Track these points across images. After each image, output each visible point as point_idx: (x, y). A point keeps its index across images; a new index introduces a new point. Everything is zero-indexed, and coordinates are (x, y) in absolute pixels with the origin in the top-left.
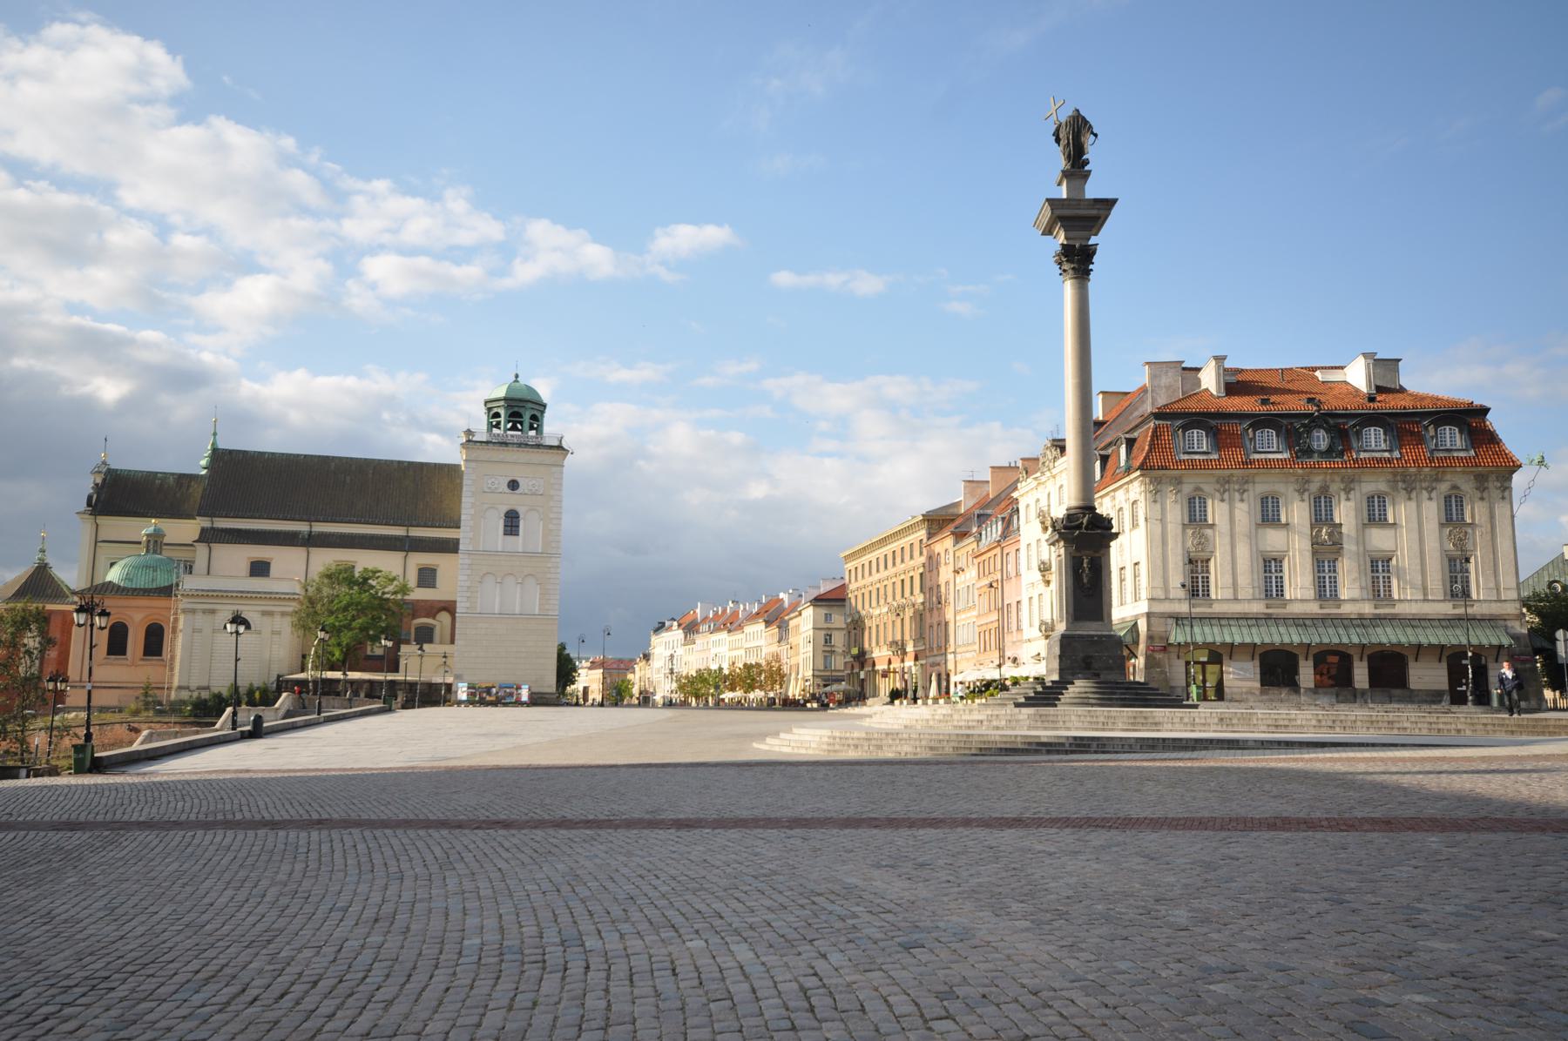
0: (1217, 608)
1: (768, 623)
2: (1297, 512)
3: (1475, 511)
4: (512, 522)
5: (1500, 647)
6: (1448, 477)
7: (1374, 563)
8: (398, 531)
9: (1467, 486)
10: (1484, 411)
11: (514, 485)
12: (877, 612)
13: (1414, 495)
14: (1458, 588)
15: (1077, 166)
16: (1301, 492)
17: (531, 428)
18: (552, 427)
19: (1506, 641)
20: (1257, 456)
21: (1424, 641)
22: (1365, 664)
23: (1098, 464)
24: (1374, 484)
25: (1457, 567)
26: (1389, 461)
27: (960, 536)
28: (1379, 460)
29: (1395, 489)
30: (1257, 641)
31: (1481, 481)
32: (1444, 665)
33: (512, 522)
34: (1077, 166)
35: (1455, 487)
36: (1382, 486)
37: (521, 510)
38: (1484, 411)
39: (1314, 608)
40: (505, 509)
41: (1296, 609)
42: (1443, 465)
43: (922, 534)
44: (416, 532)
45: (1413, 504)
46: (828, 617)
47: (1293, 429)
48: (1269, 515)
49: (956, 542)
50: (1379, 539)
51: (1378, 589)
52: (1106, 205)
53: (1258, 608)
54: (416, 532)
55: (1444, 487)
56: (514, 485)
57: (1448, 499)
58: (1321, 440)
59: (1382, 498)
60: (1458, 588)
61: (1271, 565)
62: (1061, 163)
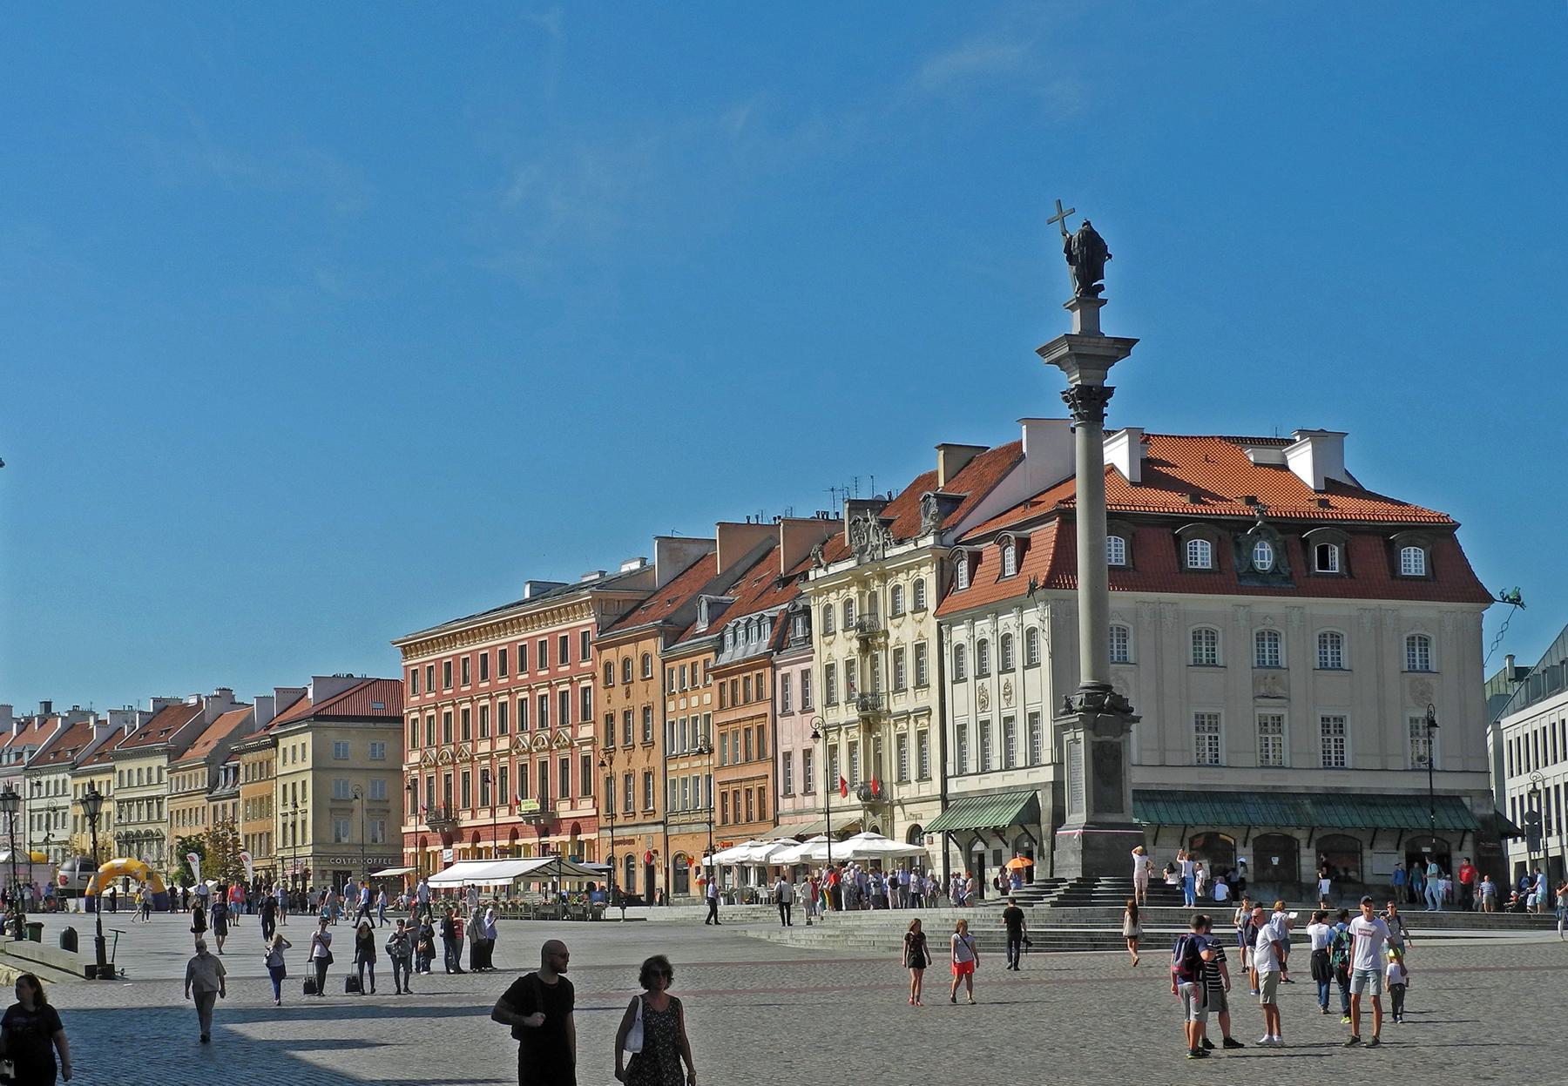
1: (175, 754)
2: (1237, 652)
5: (1466, 831)
12: (484, 747)
15: (1090, 295)
19: (1470, 825)
21: (1379, 821)
22: (1313, 851)
23: (963, 568)
27: (675, 631)
30: (1189, 821)
32: (1403, 853)
34: (1090, 295)
43: (588, 621)
49: (667, 645)
61: (1206, 723)
62: (1070, 288)
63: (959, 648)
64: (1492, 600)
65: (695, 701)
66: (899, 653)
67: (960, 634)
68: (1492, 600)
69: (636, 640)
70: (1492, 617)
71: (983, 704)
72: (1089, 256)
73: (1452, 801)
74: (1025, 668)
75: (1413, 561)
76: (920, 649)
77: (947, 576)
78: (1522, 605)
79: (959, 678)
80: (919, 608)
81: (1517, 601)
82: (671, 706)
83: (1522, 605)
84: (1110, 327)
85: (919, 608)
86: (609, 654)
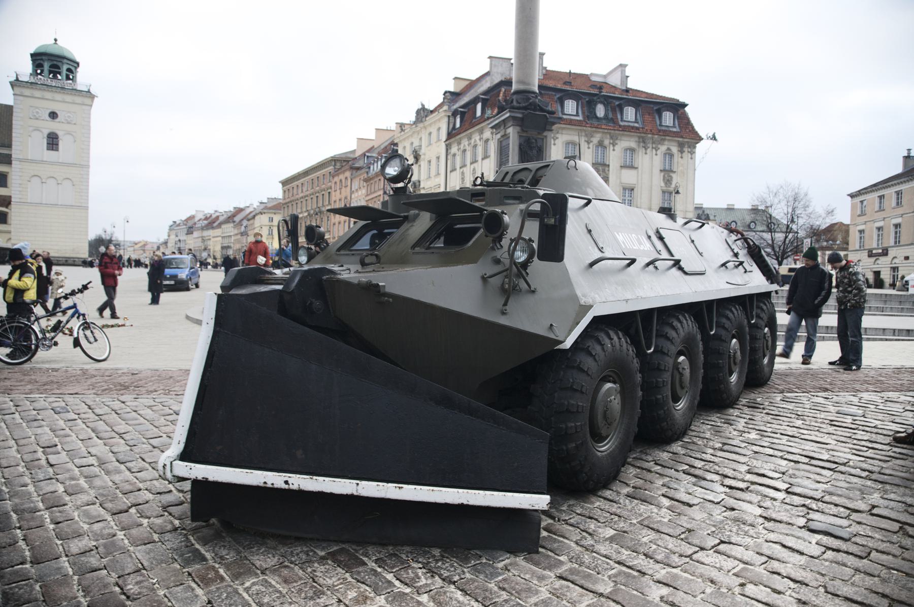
3: (679, 162)
4: (53, 141)
6: (666, 143)
7: (624, 189)
9: (675, 150)
10: (684, 105)
13: (649, 151)
16: (588, 142)
17: (68, 78)
18: (83, 78)
20: (565, 117)
26: (637, 128)
28: (633, 127)
29: (639, 146)
31: (681, 146)
33: (53, 141)
35: (669, 149)
36: (633, 144)
37: (60, 134)
38: (684, 105)
40: (46, 132)
42: (665, 133)
45: (647, 157)
50: (629, 177)
55: (663, 148)
57: (665, 154)
59: (632, 150)
63: (454, 155)
64: (701, 139)
65: (360, 193)
66: (430, 162)
67: (454, 149)
68: (701, 139)
69: (344, 172)
71: (463, 179)
74: (483, 159)
75: (668, 118)
76: (438, 158)
77: (451, 126)
78: (715, 139)
79: (454, 170)
80: (439, 140)
81: (714, 138)
82: (353, 196)
83: (715, 139)
85: (439, 140)
86: (336, 179)
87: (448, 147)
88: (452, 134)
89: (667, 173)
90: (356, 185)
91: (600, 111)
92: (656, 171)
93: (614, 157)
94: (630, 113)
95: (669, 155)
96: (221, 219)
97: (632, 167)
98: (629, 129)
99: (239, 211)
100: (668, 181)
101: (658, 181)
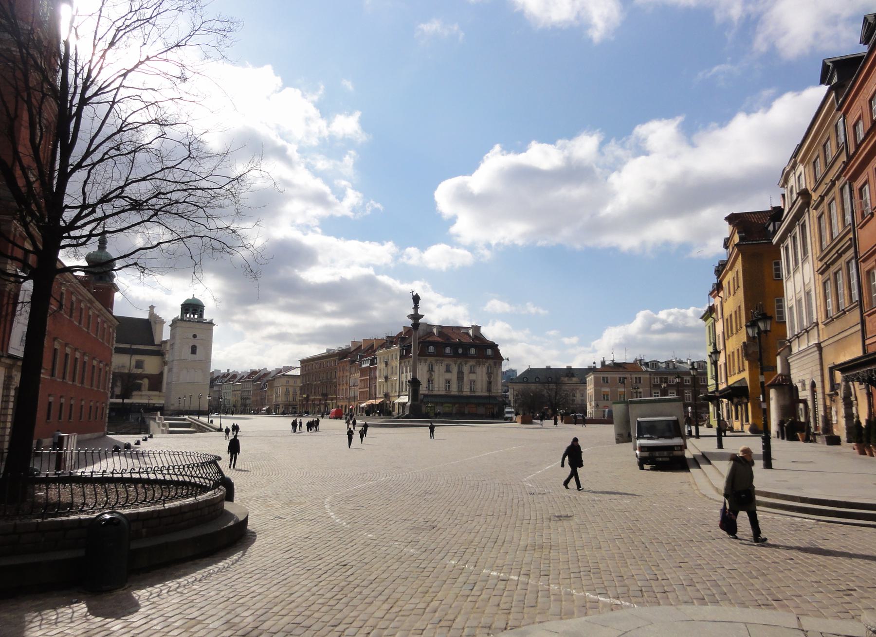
0: (435, 393)
2: (455, 369)
4: (194, 350)
8: (128, 346)
11: (195, 336)
14: (489, 390)
15: (416, 307)
18: (207, 316)
24: (472, 362)
25: (490, 383)
33: (194, 350)
34: (416, 307)
37: (197, 345)
39: (457, 393)
41: (453, 393)
44: (134, 347)
46: (288, 382)
47: (455, 346)
48: (448, 370)
50: (473, 377)
51: (472, 390)
52: (422, 316)
53: (443, 393)
54: (134, 347)
55: (487, 364)
56: (195, 336)
58: (460, 351)
60: (489, 390)
70: (504, 363)
72: (416, 299)
73: (495, 397)
75: (489, 352)
84: (420, 313)
87: (400, 363)
88: (402, 357)
89: (489, 374)
90: (353, 369)
91: (460, 351)
92: (484, 373)
93: (466, 369)
94: (473, 351)
95: (489, 367)
96: (239, 377)
97: (474, 373)
98: (472, 357)
99: (254, 373)
100: (490, 377)
101: (485, 378)
